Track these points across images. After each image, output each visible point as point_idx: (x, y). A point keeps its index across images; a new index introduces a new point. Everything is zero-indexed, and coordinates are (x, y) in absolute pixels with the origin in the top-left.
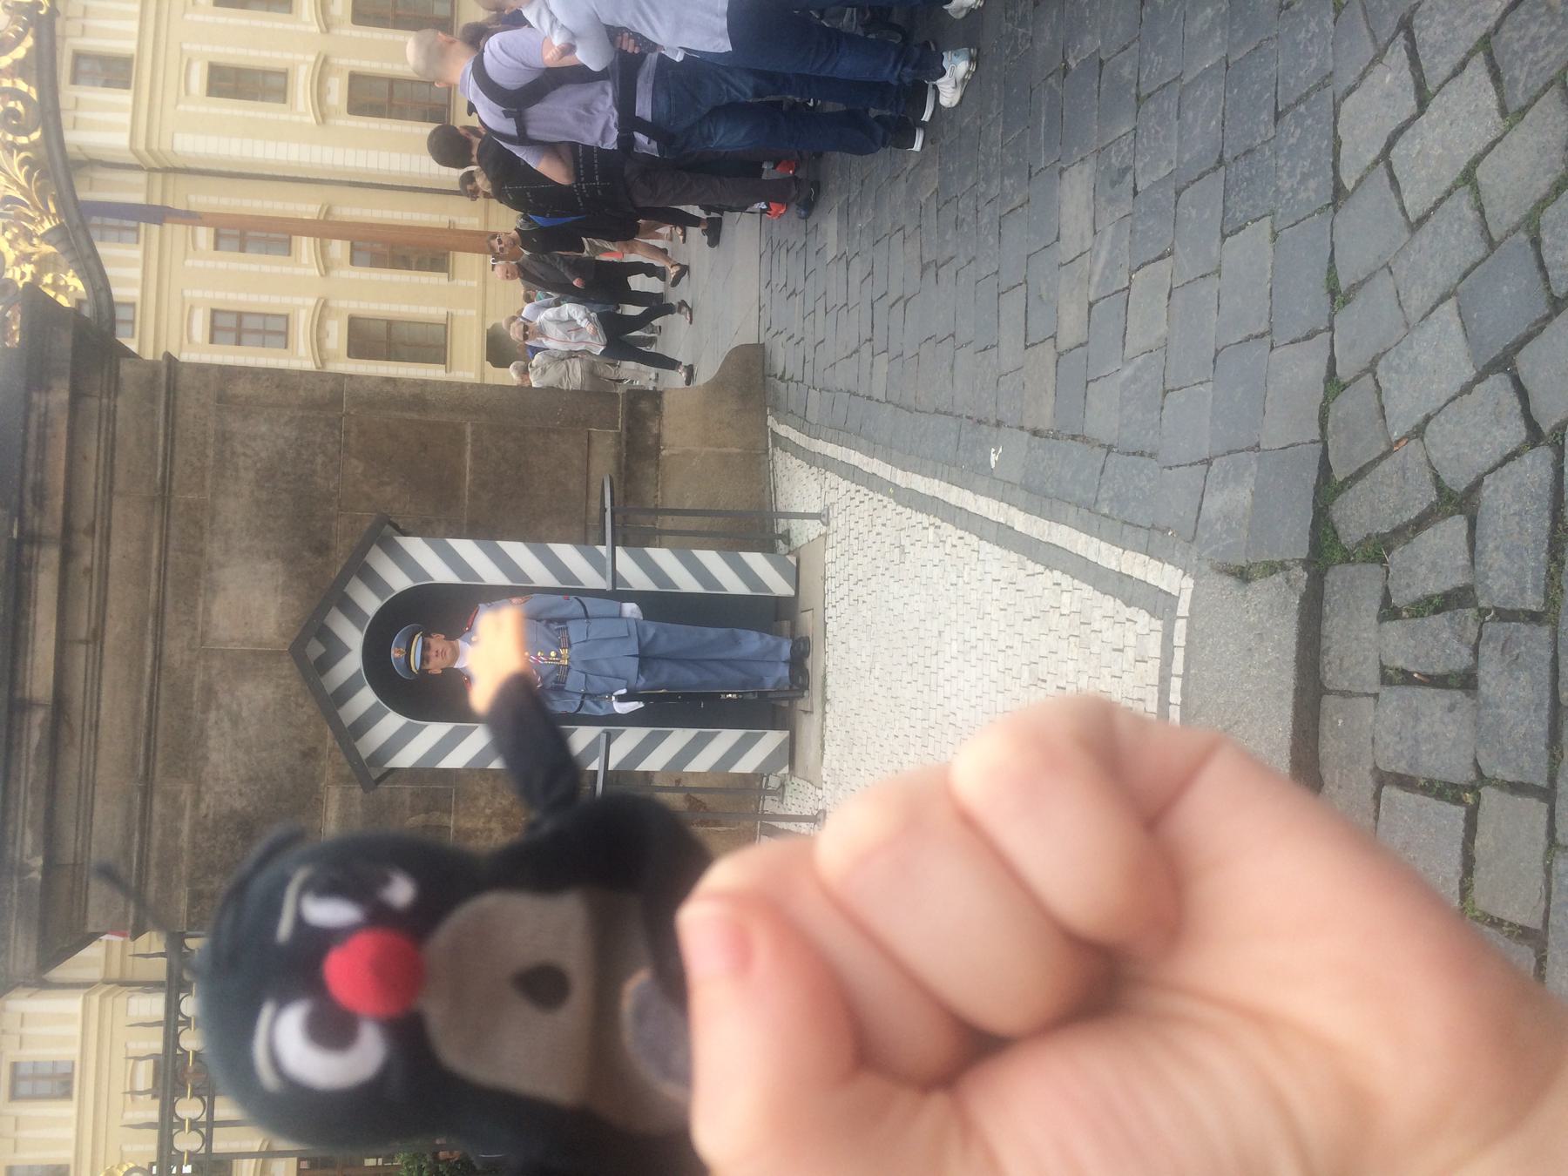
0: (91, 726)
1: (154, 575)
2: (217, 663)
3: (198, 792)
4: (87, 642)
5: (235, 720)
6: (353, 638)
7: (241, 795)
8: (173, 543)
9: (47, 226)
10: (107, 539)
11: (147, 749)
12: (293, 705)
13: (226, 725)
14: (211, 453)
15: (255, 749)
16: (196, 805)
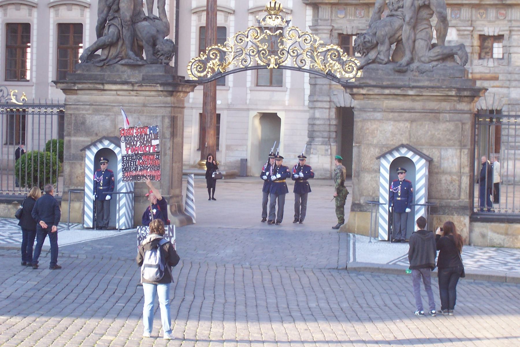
1: (130, 105)
2: (113, 117)
9: (221, 70)
10: (136, 96)
13: (102, 119)
14: (154, 114)
16: (87, 114)
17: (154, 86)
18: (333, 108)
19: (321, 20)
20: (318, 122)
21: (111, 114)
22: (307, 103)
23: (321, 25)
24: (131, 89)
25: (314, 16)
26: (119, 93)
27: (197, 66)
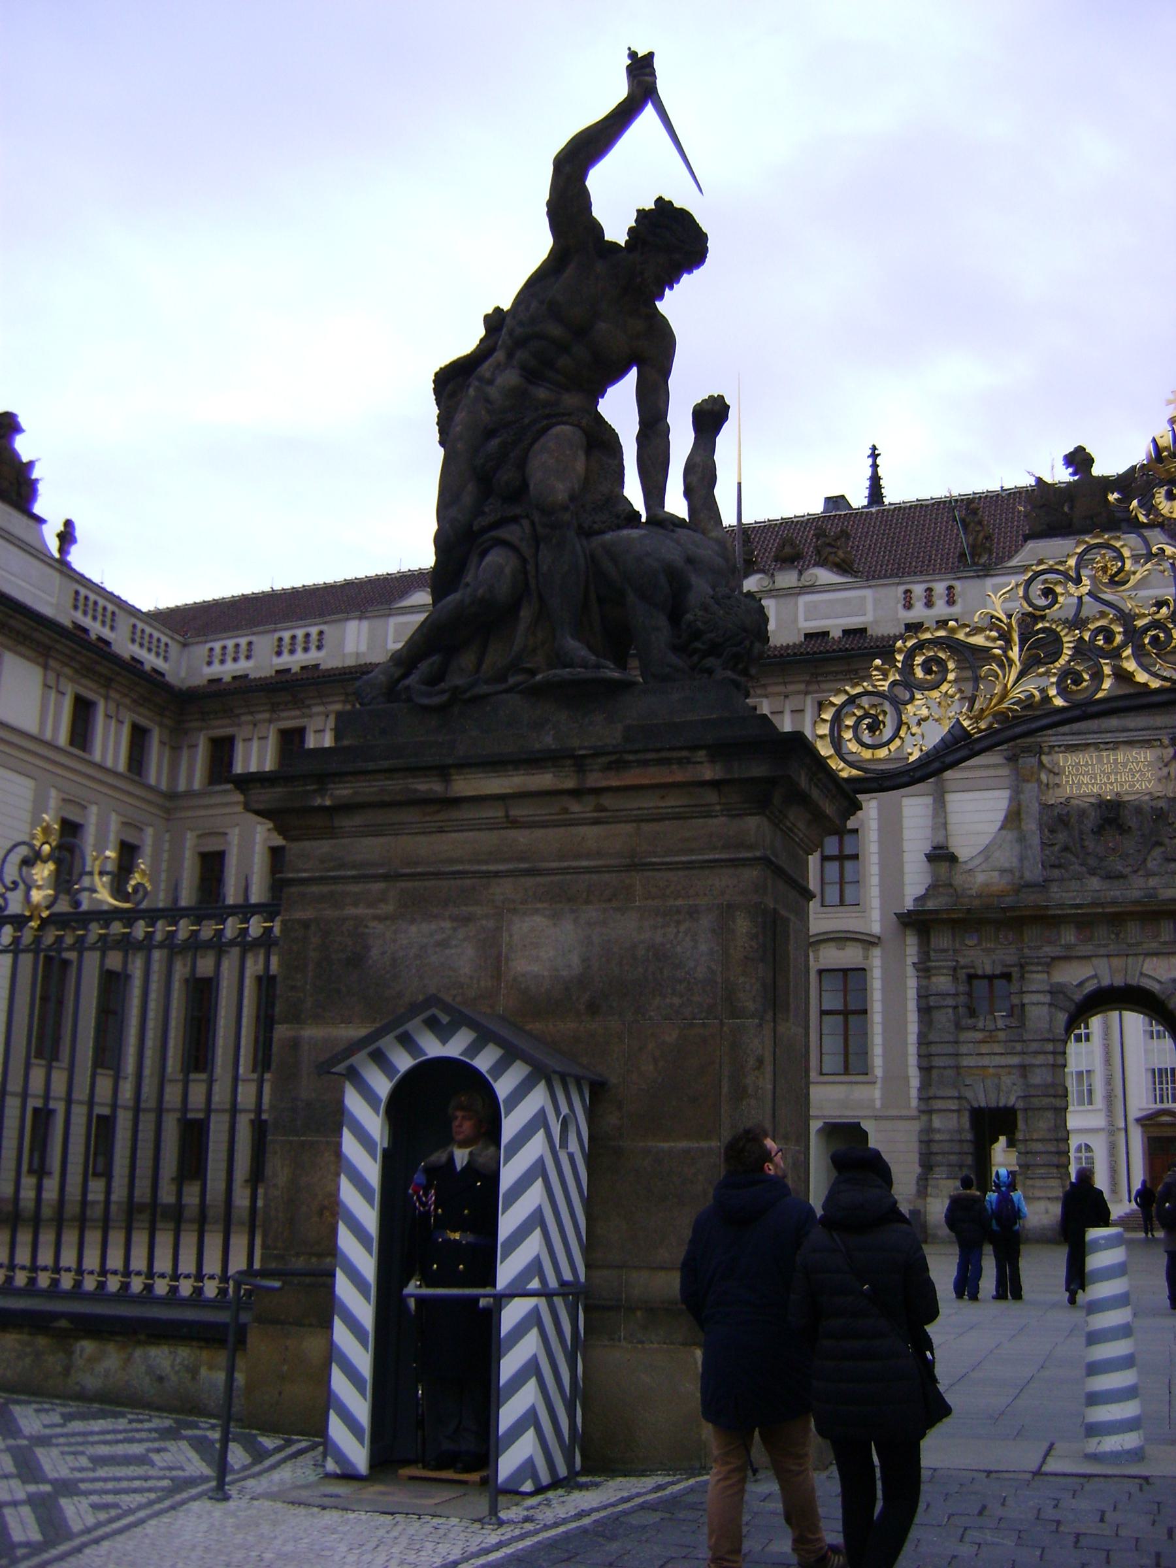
0: (441, 827)
1: (566, 864)
2: (491, 924)
3: (386, 919)
4: (507, 816)
5: (443, 944)
6: (454, 1048)
7: (383, 953)
8: (595, 877)
9: (966, 723)
10: (596, 822)
11: (420, 874)
12: (455, 992)
13: (439, 937)
14: (679, 902)
15: (418, 962)
17: (680, 762)
18: (965, 1109)
19: (935, 951)
20: (938, 1137)
21: (478, 910)
22: (914, 1103)
23: (933, 961)
24: (570, 784)
25: (920, 945)
26: (519, 811)
27: (860, 719)
